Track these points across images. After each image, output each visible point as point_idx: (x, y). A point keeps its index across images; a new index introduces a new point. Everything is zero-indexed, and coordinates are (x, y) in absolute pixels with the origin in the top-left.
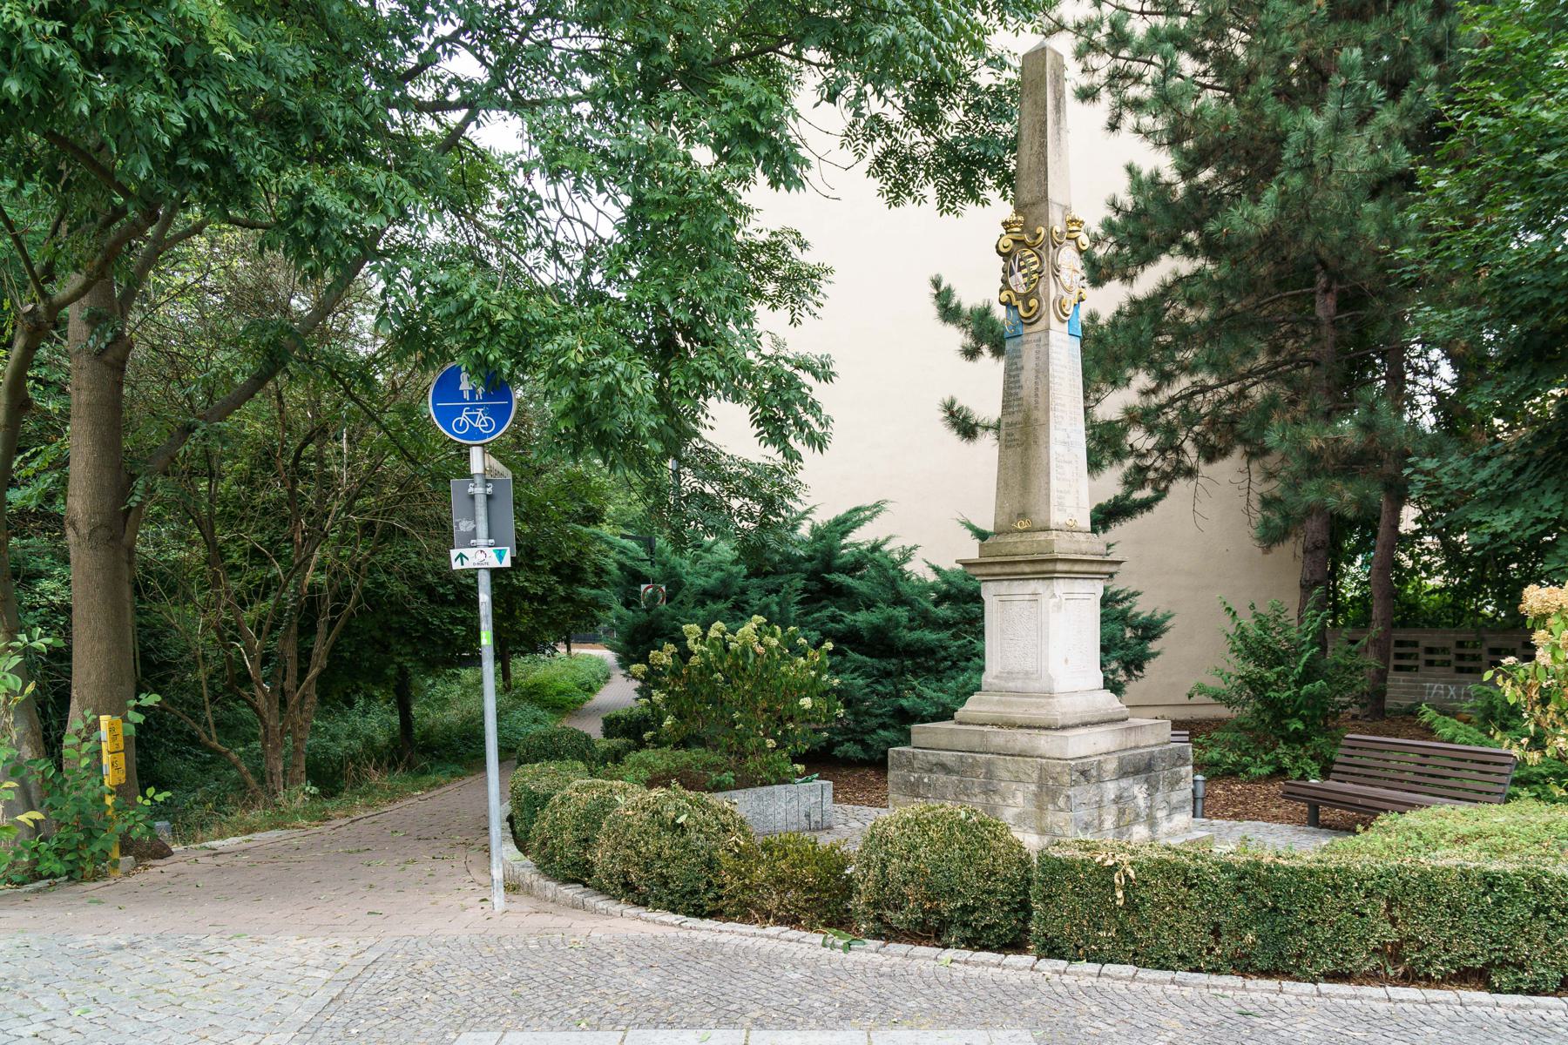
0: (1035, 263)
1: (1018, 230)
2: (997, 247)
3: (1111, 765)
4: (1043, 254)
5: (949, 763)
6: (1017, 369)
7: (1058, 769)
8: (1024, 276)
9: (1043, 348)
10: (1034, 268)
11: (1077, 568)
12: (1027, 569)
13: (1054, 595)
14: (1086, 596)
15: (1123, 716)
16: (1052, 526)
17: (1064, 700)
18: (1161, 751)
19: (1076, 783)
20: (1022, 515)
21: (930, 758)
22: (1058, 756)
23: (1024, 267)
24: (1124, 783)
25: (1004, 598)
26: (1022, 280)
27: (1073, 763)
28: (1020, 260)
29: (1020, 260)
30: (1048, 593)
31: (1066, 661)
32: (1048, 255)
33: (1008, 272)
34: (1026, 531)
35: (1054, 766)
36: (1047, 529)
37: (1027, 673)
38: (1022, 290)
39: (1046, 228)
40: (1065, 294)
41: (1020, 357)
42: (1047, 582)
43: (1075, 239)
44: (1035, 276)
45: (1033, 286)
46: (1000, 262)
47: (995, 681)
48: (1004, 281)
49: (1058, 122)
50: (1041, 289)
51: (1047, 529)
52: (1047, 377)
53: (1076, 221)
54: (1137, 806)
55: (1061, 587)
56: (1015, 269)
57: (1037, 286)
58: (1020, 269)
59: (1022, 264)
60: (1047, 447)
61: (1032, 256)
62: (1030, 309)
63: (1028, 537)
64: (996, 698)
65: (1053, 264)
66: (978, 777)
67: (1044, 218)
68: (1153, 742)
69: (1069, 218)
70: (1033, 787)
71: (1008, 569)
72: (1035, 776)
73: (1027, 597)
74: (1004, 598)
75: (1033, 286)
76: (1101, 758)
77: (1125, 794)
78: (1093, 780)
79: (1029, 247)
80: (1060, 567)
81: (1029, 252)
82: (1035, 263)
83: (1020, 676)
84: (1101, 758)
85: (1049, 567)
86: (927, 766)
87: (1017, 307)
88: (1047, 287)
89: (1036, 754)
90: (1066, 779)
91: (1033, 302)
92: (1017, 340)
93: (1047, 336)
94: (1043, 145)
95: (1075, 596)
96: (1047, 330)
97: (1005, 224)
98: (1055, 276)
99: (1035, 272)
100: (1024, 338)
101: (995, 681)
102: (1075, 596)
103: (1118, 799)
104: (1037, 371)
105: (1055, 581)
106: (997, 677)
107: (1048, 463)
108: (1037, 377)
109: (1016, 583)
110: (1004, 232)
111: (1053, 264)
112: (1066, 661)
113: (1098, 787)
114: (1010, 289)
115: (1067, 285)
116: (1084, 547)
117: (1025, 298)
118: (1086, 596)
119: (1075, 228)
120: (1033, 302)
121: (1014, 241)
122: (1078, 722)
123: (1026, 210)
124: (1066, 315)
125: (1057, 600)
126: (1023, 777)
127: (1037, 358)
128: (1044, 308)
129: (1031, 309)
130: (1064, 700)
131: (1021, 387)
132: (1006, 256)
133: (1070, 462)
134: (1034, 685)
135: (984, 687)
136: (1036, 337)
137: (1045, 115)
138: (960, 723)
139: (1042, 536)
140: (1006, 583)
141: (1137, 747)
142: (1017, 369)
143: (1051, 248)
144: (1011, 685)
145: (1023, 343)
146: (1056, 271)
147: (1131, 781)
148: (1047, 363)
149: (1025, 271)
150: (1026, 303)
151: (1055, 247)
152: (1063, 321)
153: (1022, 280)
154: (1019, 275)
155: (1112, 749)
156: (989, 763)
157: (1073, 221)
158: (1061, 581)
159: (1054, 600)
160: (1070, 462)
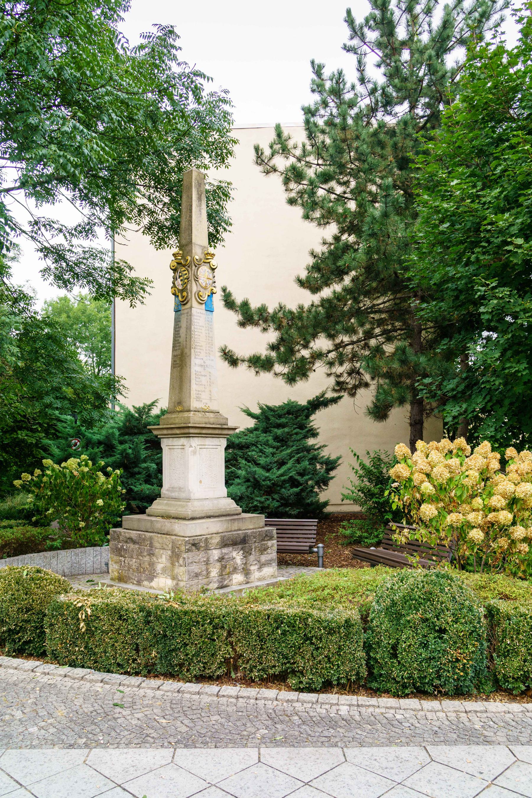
3: (216, 540)
5: (134, 538)
7: (180, 543)
8: (181, 280)
10: (185, 276)
11: (204, 431)
12: (178, 431)
13: (191, 446)
15: (237, 512)
16: (192, 409)
17: (196, 503)
19: (188, 550)
21: (127, 535)
22: (183, 535)
24: (225, 550)
27: (187, 539)
30: (188, 445)
31: (201, 482)
33: (175, 279)
34: (181, 411)
35: (178, 541)
38: (180, 288)
40: (202, 290)
42: (188, 439)
43: (209, 263)
44: (186, 281)
46: (171, 273)
48: (174, 283)
50: (188, 287)
51: (189, 411)
55: (195, 442)
58: (180, 277)
60: (190, 368)
63: (181, 415)
64: (165, 502)
65: (194, 275)
66: (146, 546)
67: (190, 252)
68: (251, 527)
69: (206, 252)
70: (169, 552)
71: (170, 432)
72: (170, 546)
73: (180, 447)
76: (208, 536)
77: (226, 557)
79: (184, 266)
80: (192, 431)
81: (184, 269)
83: (177, 489)
85: (186, 431)
86: (125, 539)
88: (191, 286)
89: (174, 533)
90: (183, 548)
94: (191, 216)
95: (206, 447)
96: (191, 307)
97: (174, 255)
98: (195, 280)
100: (182, 312)
102: (206, 447)
103: (221, 559)
104: (187, 329)
105: (191, 439)
109: (175, 439)
110: (174, 259)
111: (194, 275)
112: (201, 482)
113: (206, 553)
114: (176, 287)
115: (204, 285)
116: (212, 420)
117: (182, 291)
120: (185, 294)
121: (178, 263)
122: (203, 515)
125: (193, 449)
126: (165, 547)
128: (189, 297)
130: (196, 503)
131: (180, 337)
132: (175, 270)
134: (183, 495)
135: (162, 496)
138: (149, 515)
139: (186, 414)
140: (171, 439)
141: (240, 530)
143: (194, 267)
145: (181, 314)
148: (191, 324)
149: (181, 278)
153: (180, 283)
154: (179, 280)
155: (220, 531)
156: (151, 538)
158: (196, 439)
159: (191, 449)
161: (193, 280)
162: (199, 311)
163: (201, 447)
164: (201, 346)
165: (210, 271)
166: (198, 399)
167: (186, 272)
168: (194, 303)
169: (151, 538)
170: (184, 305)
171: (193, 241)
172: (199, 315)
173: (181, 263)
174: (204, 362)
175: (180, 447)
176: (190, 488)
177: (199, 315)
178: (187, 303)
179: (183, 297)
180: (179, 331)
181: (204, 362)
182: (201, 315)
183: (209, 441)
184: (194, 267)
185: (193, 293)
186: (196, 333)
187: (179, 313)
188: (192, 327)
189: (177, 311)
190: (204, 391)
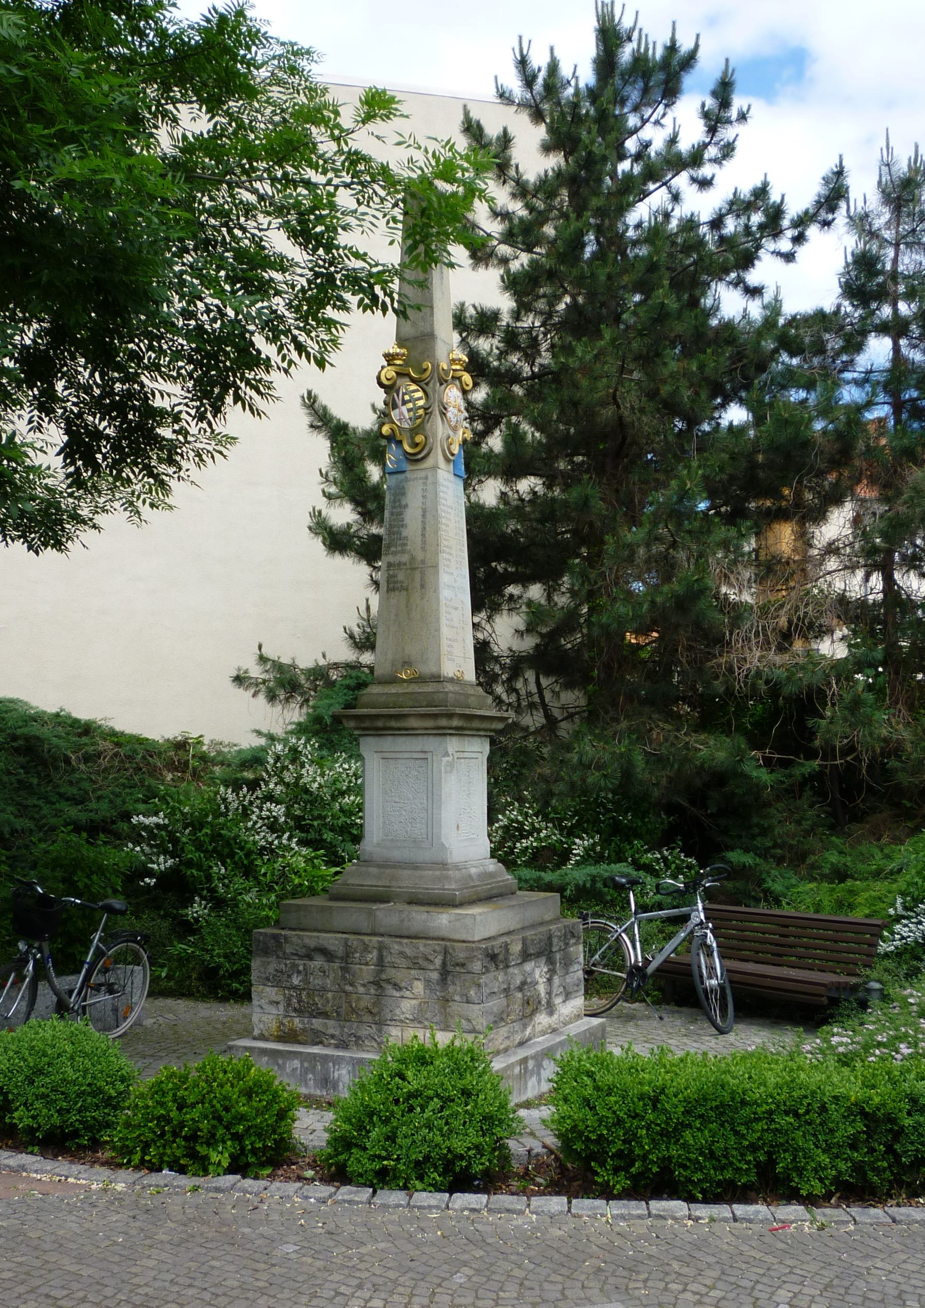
2: (379, 378)
4: (429, 390)
5: (331, 948)
8: (409, 410)
9: (430, 487)
10: (421, 403)
13: (446, 754)
14: (474, 755)
21: (307, 941)
23: (409, 401)
29: (404, 394)
41: (404, 494)
45: (419, 421)
56: (399, 403)
58: (404, 403)
60: (436, 590)
66: (367, 964)
67: (429, 353)
70: (435, 976)
72: (438, 961)
75: (419, 421)
86: (302, 951)
91: (419, 439)
92: (401, 477)
96: (435, 467)
99: (420, 408)
100: (408, 474)
104: (424, 511)
105: (448, 738)
106: (378, 845)
107: (438, 610)
108: (424, 516)
110: (385, 363)
118: (474, 755)
120: (419, 439)
124: (453, 455)
125: (450, 759)
129: (417, 445)
132: (389, 388)
133: (456, 609)
140: (390, 739)
145: (407, 480)
149: (410, 405)
151: (441, 384)
159: (445, 759)
160: (456, 609)
169: (381, 948)
173: (408, 375)
176: (443, 840)
180: (401, 514)
188: (440, 507)
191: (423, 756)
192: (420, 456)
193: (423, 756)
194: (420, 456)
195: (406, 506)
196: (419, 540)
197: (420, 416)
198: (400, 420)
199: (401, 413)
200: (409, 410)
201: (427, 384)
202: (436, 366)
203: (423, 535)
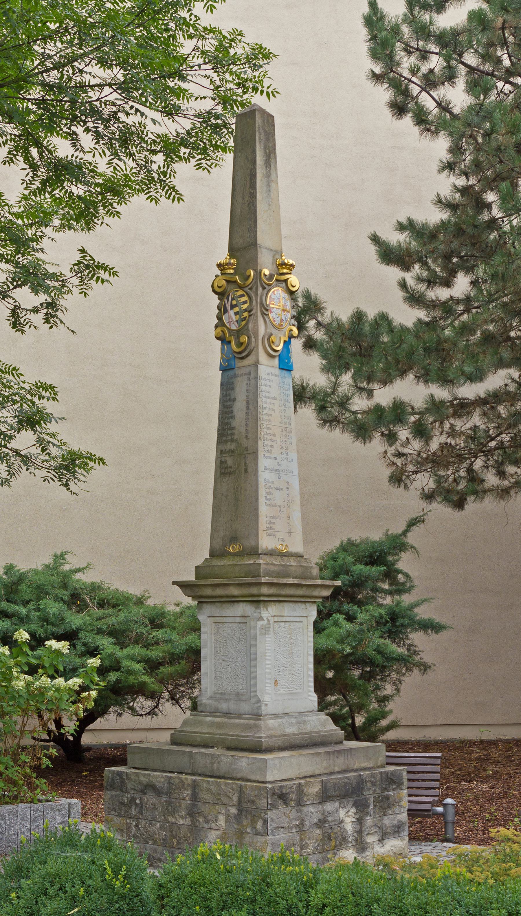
0: (245, 302)
1: (231, 271)
2: (212, 286)
3: (314, 789)
5: (158, 785)
6: (230, 400)
8: (236, 314)
9: (253, 382)
10: (245, 306)
12: (235, 591)
13: (261, 618)
14: (298, 619)
17: (271, 723)
18: (372, 775)
19: (273, 807)
20: (234, 539)
21: (142, 778)
23: (236, 306)
24: (330, 807)
25: (217, 619)
26: (234, 318)
27: (270, 786)
28: (233, 299)
29: (233, 299)
32: (256, 294)
33: (222, 310)
36: (254, 552)
37: (238, 694)
38: (234, 327)
39: (255, 270)
40: (274, 331)
41: (233, 389)
43: (286, 281)
44: (246, 314)
45: (244, 323)
46: (215, 300)
47: (210, 702)
48: (219, 318)
49: (268, 176)
50: (251, 326)
52: (256, 407)
53: (285, 264)
54: (344, 831)
56: (229, 307)
57: (247, 324)
58: (233, 307)
59: (234, 302)
61: (242, 296)
62: (241, 344)
67: (253, 262)
69: (279, 261)
70: (233, 811)
72: (235, 798)
73: (238, 620)
74: (217, 619)
75: (244, 323)
77: (330, 819)
78: (293, 803)
79: (241, 287)
81: (241, 292)
82: (245, 302)
84: (302, 781)
87: (229, 342)
88: (256, 325)
89: (239, 775)
90: (263, 803)
91: (244, 339)
93: (257, 371)
94: (253, 196)
95: (284, 619)
96: (256, 364)
97: (219, 266)
98: (263, 314)
99: (245, 310)
100: (237, 372)
101: (210, 702)
102: (284, 619)
103: (321, 823)
104: (248, 403)
106: (211, 698)
108: (247, 408)
110: (219, 273)
111: (262, 304)
112: (276, 683)
113: (299, 811)
114: (224, 325)
115: (277, 322)
117: (238, 333)
118: (298, 619)
119: (285, 271)
120: (244, 339)
123: (238, 254)
124: (276, 351)
125: (265, 622)
127: (248, 391)
128: (253, 345)
129: (242, 344)
130: (271, 723)
131: (233, 417)
132: (221, 294)
133: (280, 489)
136: (247, 370)
137: (255, 169)
142: (230, 400)
143: (260, 290)
144: (224, 706)
145: (235, 376)
146: (265, 310)
147: (337, 804)
149: (237, 309)
150: (238, 338)
151: (264, 288)
152: (273, 357)
153: (234, 318)
155: (317, 772)
157: (284, 264)
159: (260, 623)
160: (280, 489)
161: (259, 314)
162: (269, 370)
163: (276, 619)
164: (274, 435)
165: (287, 296)
166: (271, 532)
167: (245, 298)
168: (263, 357)
169: (195, 785)
170: (242, 358)
171: (259, 242)
172: (270, 377)
173: (235, 282)
174: (279, 465)
175: (238, 620)
176: (258, 694)
177: (270, 377)
178: (247, 356)
179: (240, 344)
180: (230, 407)
181: (279, 465)
182: (273, 378)
183: (287, 610)
184: (260, 290)
185: (260, 338)
186: (265, 411)
187: (231, 373)
188: (260, 400)
189: (225, 369)
190: (280, 518)
191: (243, 620)
192: (244, 354)
193: (243, 620)
194: (244, 354)
195: (234, 400)
196: (243, 430)
197: (245, 318)
198: (229, 322)
199: (230, 317)
200: (236, 314)
201: (251, 289)
202: (259, 273)
203: (247, 425)
